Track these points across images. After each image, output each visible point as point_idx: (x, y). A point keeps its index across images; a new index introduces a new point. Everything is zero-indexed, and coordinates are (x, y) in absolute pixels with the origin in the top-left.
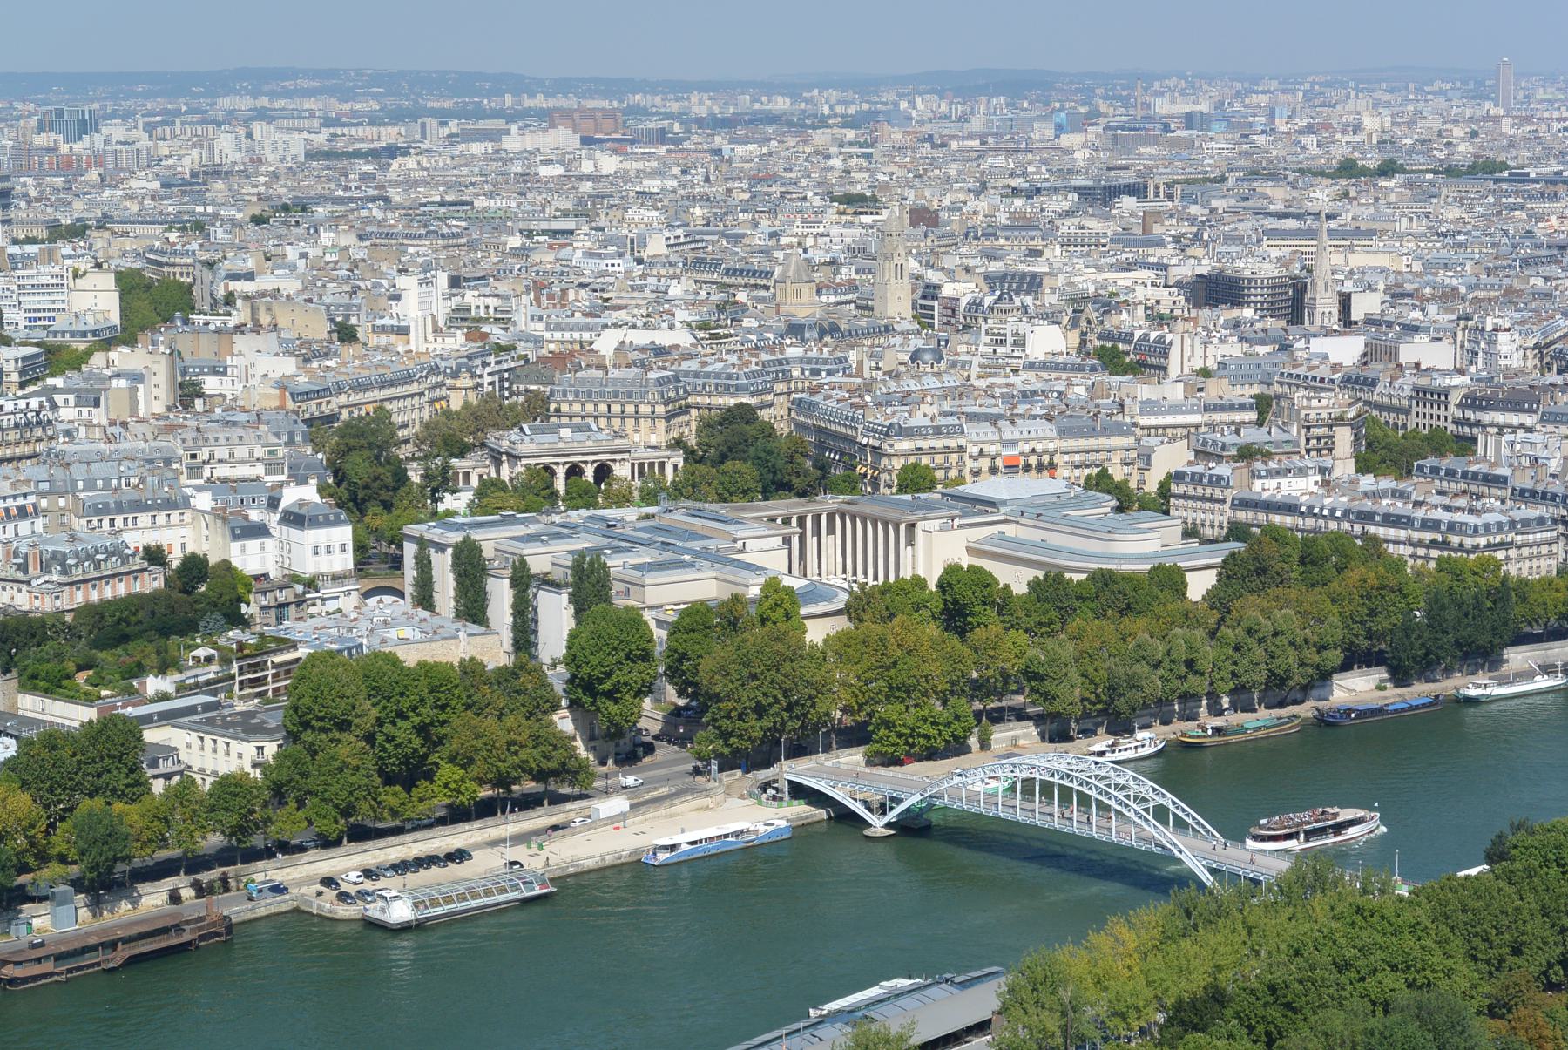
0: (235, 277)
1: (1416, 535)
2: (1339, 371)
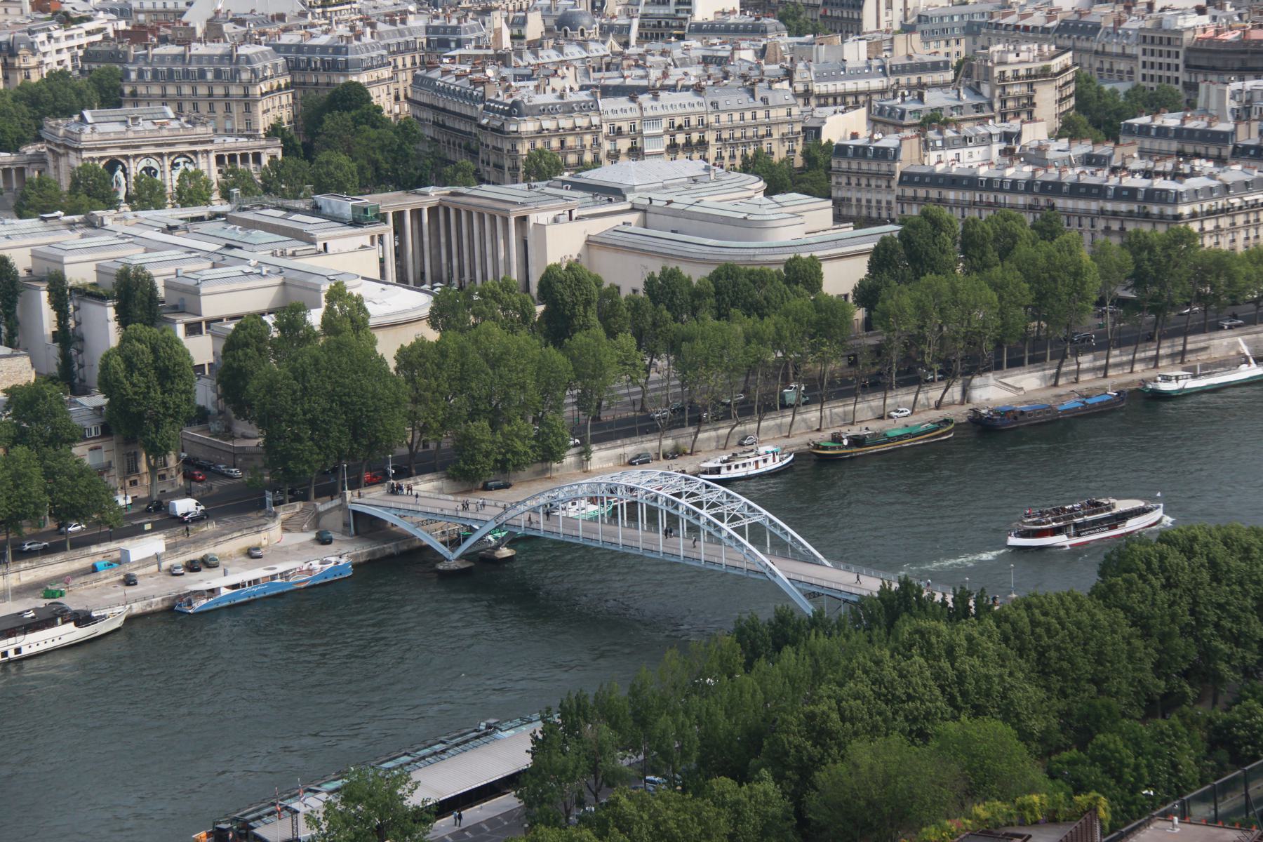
1: (1109, 206)
2: (1055, 18)
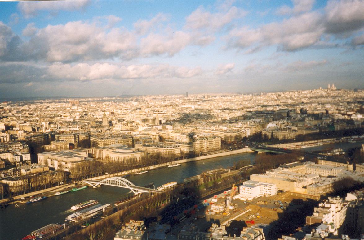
0: (20, 123)
1: (164, 148)
